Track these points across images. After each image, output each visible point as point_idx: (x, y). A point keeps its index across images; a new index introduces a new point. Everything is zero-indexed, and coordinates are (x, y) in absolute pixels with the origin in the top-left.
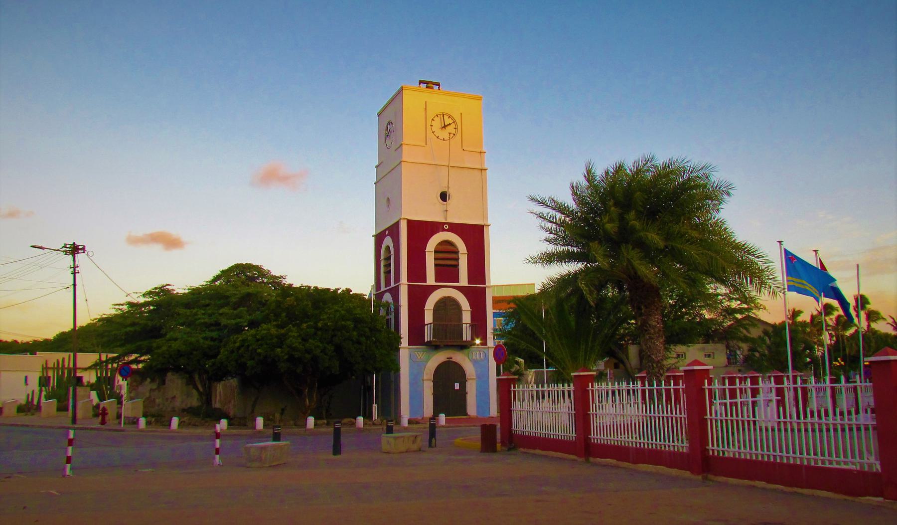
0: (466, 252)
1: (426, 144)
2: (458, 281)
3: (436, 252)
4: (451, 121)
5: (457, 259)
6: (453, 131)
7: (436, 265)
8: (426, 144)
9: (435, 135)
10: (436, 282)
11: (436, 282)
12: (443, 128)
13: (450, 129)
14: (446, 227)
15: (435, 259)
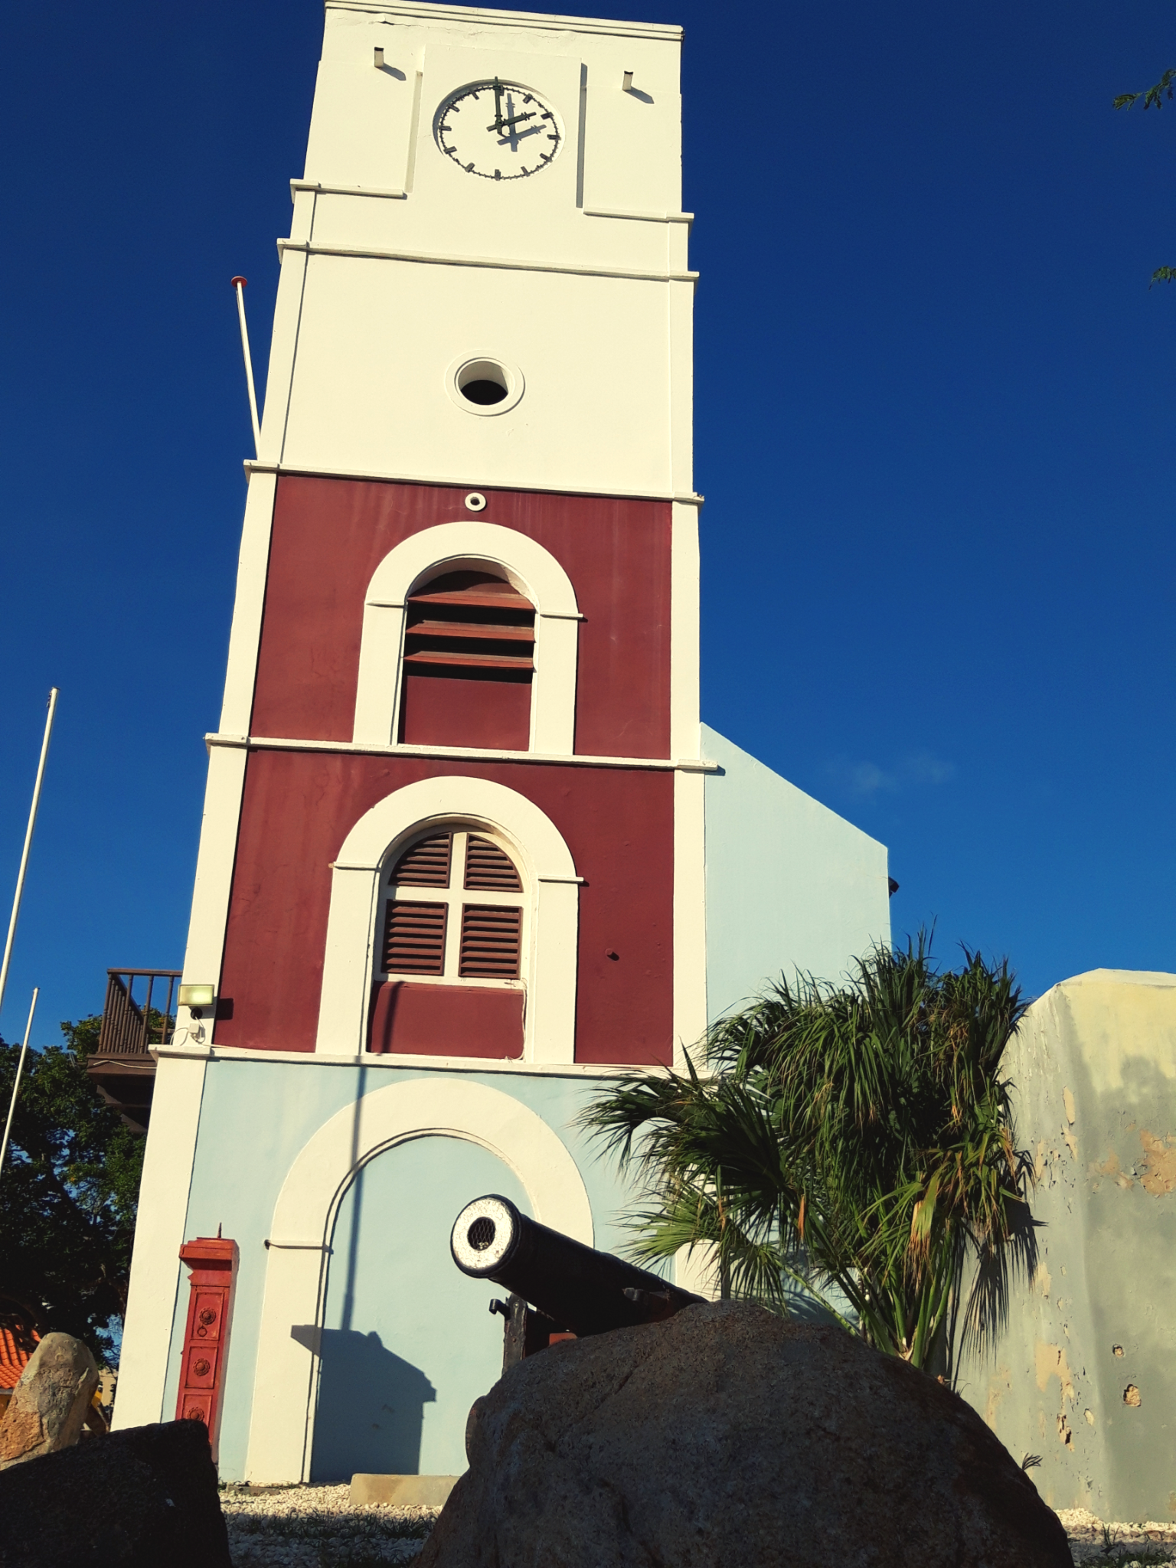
0: (575, 612)
1: (409, 184)
2: (524, 746)
3: (415, 611)
4: (531, 108)
5: (526, 648)
6: (547, 146)
7: (410, 670)
8: (409, 184)
9: (457, 161)
10: (401, 740)
11: (401, 740)
12: (490, 129)
13: (532, 148)
14: (475, 502)
15: (412, 643)
